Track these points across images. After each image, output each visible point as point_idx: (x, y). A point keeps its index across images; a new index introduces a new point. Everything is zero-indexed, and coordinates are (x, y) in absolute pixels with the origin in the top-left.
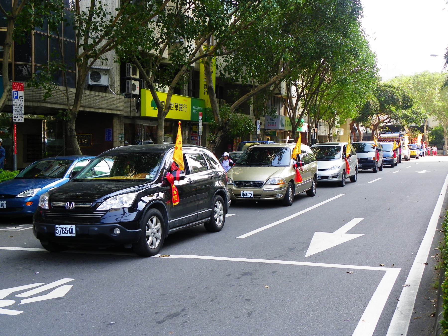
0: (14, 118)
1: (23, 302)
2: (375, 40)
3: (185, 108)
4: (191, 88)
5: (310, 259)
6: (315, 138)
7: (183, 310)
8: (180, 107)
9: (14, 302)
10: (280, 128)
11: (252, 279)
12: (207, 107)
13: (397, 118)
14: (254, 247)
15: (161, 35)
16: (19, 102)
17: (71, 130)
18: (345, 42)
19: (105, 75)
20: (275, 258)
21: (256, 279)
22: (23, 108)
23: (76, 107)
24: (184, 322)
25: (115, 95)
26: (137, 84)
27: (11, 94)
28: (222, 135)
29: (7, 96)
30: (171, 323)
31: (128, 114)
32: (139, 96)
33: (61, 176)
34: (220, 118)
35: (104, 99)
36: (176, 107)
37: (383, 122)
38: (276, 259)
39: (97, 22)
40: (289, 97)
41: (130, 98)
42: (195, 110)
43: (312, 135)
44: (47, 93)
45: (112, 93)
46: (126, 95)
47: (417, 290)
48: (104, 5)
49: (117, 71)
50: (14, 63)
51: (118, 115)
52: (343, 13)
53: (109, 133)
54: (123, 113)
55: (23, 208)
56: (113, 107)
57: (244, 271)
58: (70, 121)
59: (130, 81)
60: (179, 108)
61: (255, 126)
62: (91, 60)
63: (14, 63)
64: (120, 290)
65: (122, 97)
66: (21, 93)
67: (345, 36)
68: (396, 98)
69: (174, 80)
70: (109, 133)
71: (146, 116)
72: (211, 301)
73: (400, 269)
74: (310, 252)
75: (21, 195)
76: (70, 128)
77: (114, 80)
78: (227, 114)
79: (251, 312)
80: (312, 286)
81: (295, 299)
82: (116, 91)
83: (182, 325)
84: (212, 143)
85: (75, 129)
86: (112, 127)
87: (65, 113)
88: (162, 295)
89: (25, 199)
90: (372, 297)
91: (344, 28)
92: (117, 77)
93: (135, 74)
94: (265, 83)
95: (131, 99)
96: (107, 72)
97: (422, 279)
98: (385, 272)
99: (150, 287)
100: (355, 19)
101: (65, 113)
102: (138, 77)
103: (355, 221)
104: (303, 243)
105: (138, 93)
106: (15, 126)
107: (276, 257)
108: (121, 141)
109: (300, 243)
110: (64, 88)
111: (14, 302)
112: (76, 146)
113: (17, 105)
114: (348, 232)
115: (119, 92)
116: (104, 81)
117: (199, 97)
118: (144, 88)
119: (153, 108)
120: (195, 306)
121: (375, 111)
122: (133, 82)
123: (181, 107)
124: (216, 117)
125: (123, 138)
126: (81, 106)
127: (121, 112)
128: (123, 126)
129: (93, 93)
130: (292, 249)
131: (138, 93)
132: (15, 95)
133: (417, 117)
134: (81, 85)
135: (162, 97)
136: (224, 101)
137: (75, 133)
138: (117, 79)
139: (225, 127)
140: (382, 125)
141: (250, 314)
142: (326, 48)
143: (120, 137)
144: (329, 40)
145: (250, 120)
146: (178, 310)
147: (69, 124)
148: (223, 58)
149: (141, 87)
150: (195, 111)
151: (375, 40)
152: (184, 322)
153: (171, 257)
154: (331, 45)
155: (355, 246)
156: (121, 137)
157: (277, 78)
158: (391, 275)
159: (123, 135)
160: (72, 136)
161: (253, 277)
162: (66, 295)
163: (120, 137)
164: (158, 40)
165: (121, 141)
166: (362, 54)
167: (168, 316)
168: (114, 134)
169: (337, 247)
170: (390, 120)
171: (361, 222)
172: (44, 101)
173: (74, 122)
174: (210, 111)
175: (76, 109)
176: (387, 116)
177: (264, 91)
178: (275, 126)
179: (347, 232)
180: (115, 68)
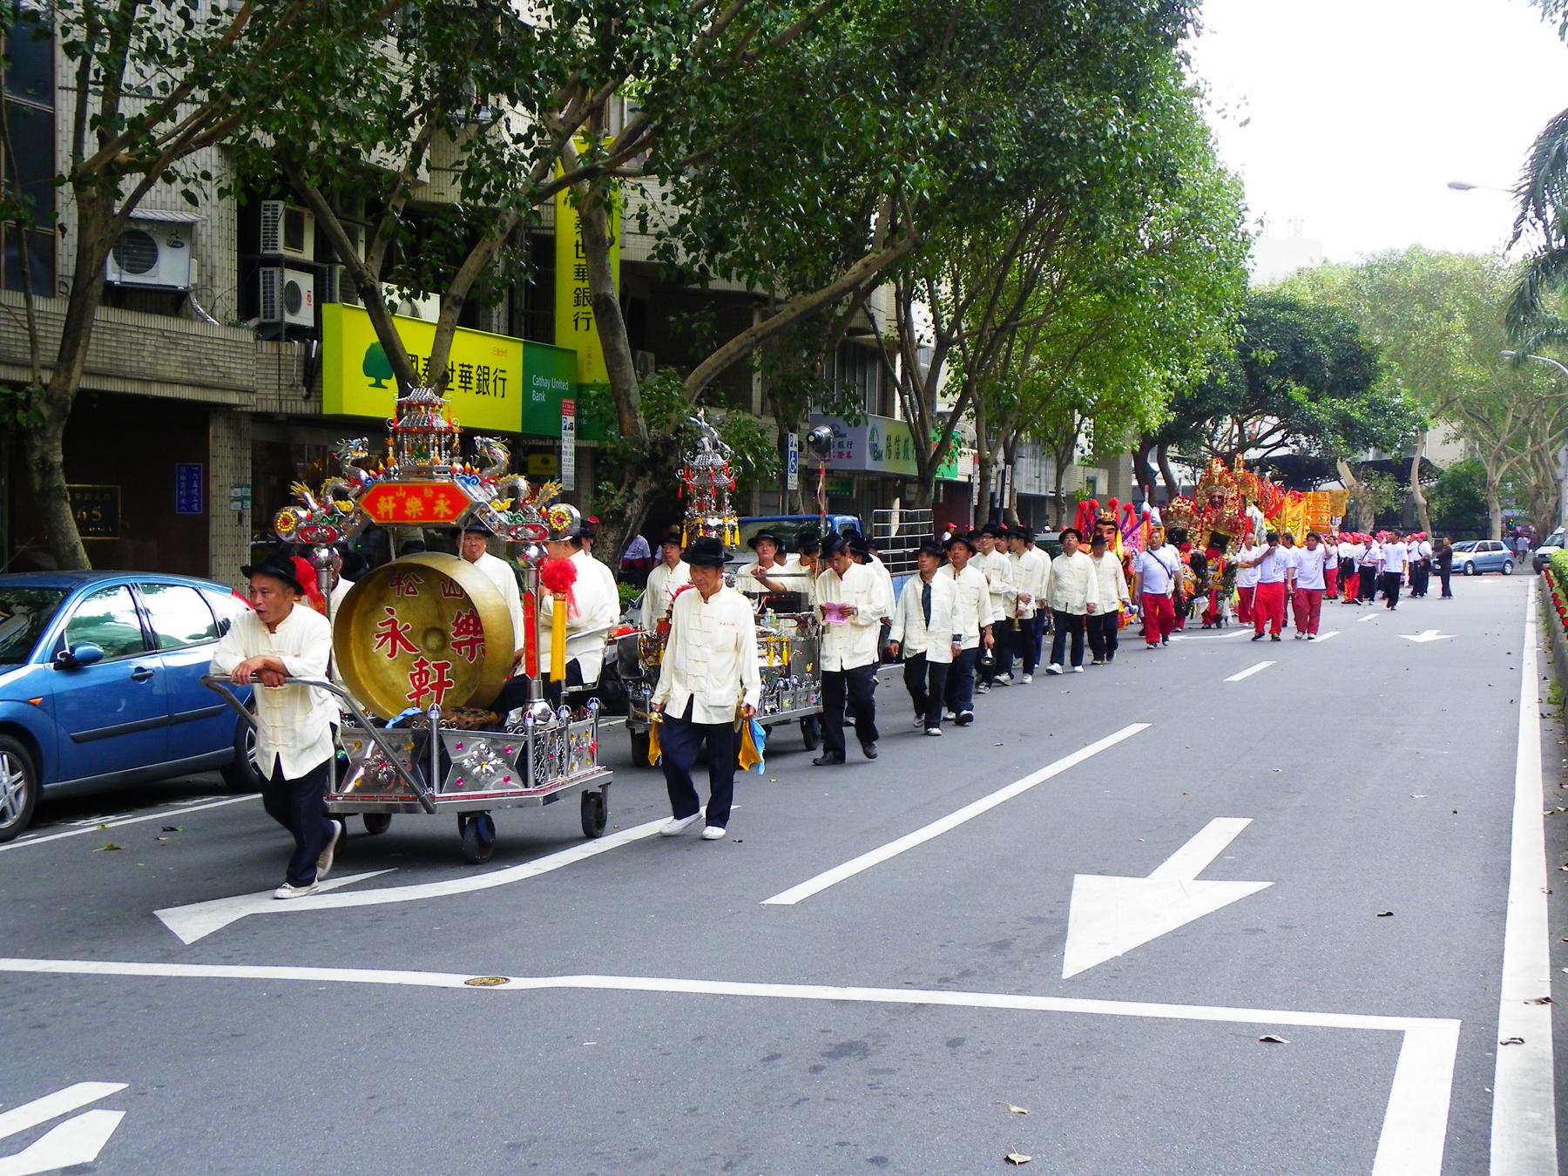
2: (1247, 121)
3: (500, 383)
5: (1085, 984)
6: (1006, 506)
8: (481, 380)
10: (870, 464)
11: (873, 1071)
12: (588, 379)
14: (839, 937)
15: (417, 88)
17: (47, 469)
18: (1135, 129)
19: (176, 245)
20: (944, 983)
21: (891, 1071)
23: (69, 371)
26: (306, 283)
28: (652, 492)
31: (270, 406)
32: (316, 332)
33: (18, 654)
34: (641, 421)
35: (172, 340)
36: (466, 378)
37: (1257, 443)
38: (948, 989)
39: (161, 27)
40: (905, 340)
41: (275, 338)
42: (539, 390)
43: (993, 495)
45: (205, 320)
47: (1553, 1109)
49: (225, 233)
51: (226, 409)
53: (189, 487)
56: (208, 375)
58: (41, 431)
59: (276, 271)
60: (474, 382)
61: (776, 459)
62: (130, 183)
64: (331, 1129)
65: (249, 337)
67: (1133, 105)
69: (462, 271)
70: (189, 482)
72: (725, 1169)
74: (1078, 957)
76: (44, 460)
77: (213, 267)
78: (671, 408)
81: (1069, 1154)
82: (219, 312)
84: (612, 522)
85: (65, 464)
86: (204, 456)
87: (21, 395)
88: (514, 1145)
90: (1381, 1142)
91: (1128, 73)
93: (295, 241)
94: (819, 286)
95: (283, 345)
96: (181, 234)
97: (1556, 1062)
98: (1399, 1035)
99: (456, 1115)
100: (1171, 41)
101: (21, 395)
102: (308, 254)
103: (1220, 833)
104: (1040, 920)
105: (310, 323)
108: (240, 515)
109: (1029, 919)
110: (16, 299)
112: (66, 535)
115: (234, 316)
116: (171, 269)
118: (331, 301)
119: (373, 381)
122: (290, 276)
123: (487, 378)
124: (627, 418)
126: (87, 373)
127: (244, 396)
128: (249, 454)
129: (130, 318)
130: (1002, 946)
131: (310, 323)
133: (1389, 424)
134: (91, 281)
135: (416, 340)
136: (651, 357)
137: (60, 480)
138: (225, 262)
139: (665, 460)
140: (1253, 454)
143: (237, 499)
144: (1074, 118)
147: (38, 442)
149: (322, 296)
150: (538, 397)
151: (1247, 121)
153: (516, 983)
154: (1083, 140)
155: (1251, 932)
156: (242, 499)
157: (866, 266)
159: (248, 492)
160: (50, 493)
162: (103, 1152)
163: (237, 499)
165: (240, 515)
166: (1192, 178)
168: (213, 487)
169: (1179, 933)
170: (1284, 438)
173: (60, 434)
174: (600, 395)
175: (68, 380)
176: (1275, 420)
177: (813, 317)
178: (849, 456)
179: (1205, 875)
180: (215, 219)
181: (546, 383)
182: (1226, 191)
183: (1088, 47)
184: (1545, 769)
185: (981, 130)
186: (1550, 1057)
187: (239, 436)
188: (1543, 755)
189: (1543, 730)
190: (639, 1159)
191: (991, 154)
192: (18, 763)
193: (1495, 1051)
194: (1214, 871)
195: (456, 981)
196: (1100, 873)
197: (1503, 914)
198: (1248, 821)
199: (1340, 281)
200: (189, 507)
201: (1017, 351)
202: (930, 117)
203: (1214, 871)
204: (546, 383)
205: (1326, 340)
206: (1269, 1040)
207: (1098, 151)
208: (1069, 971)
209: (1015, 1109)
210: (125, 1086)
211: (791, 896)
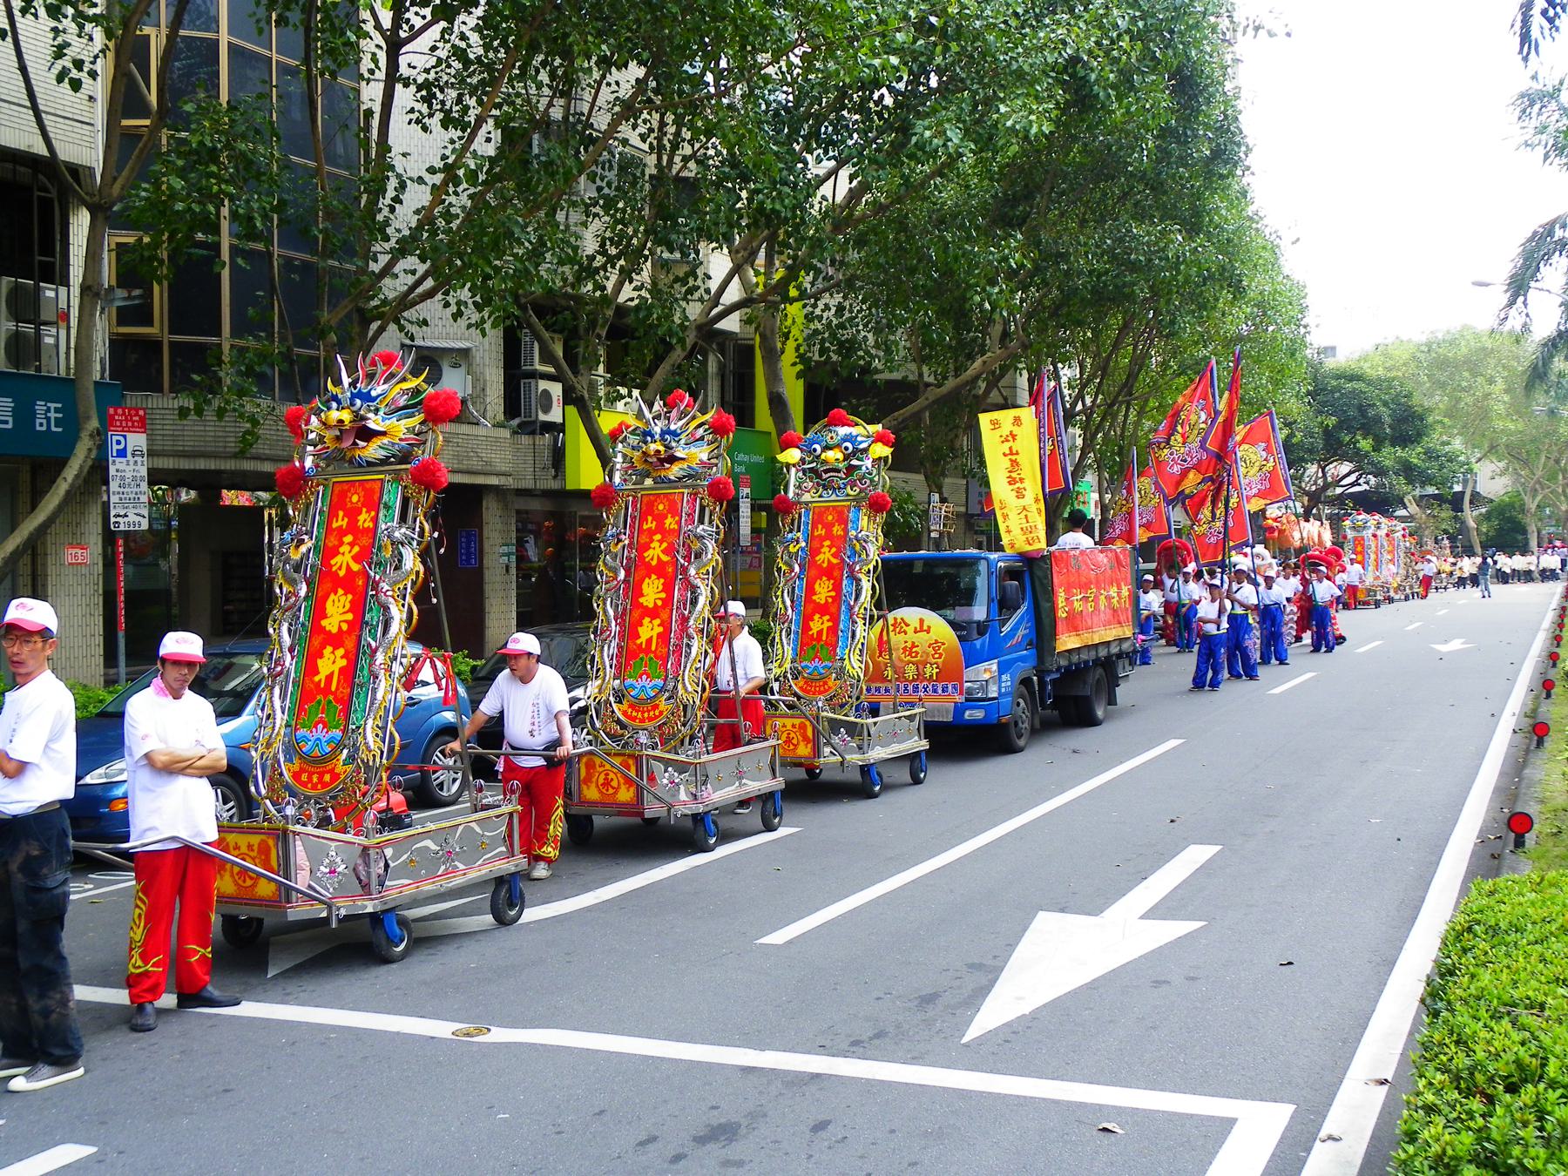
0: (113, 520)
4: (730, 397)
11: (727, 1163)
13: (1380, 472)
15: (603, 245)
16: (132, 467)
19: (456, 366)
20: (856, 1048)
21: (740, 1164)
22: (144, 486)
25: (486, 429)
26: (556, 390)
27: (103, 447)
29: (90, 450)
37: (1337, 483)
41: (533, 433)
42: (740, 463)
44: (247, 432)
46: (519, 426)
48: (404, 155)
50: (167, 338)
51: (496, 487)
52: (1182, 161)
53: (468, 543)
54: (509, 482)
55: (101, 817)
56: (475, 464)
57: (717, 1119)
59: (533, 381)
62: (374, 326)
65: (506, 433)
66: (137, 440)
67: (1193, 227)
68: (1371, 413)
71: (583, 487)
73: (1289, 1109)
74: (994, 1013)
75: (100, 776)
82: (489, 414)
89: (110, 790)
92: (494, 370)
94: (956, 376)
96: (462, 356)
98: (1230, 1123)
103: (1197, 855)
106: (121, 542)
107: (855, 1043)
109: (971, 966)
113: (123, 478)
114: (1153, 913)
116: (454, 382)
117: (752, 425)
121: (1311, 451)
122: (543, 385)
125: (513, 558)
130: (929, 999)
132: (115, 447)
133: (1441, 467)
142: (1132, 271)
143: (504, 555)
145: (909, 493)
148: (804, 306)
149: (569, 398)
153: (499, 1035)
155: (1158, 983)
156: (508, 555)
161: (736, 1150)
163: (504, 555)
164: (592, 258)
166: (1256, 285)
171: (1205, 869)
172: (240, 455)
180: (488, 349)
181: (746, 458)
183: (1157, 187)
184: (1497, 790)
185: (1061, 255)
186: (1358, 1161)
187: (506, 507)
188: (1502, 774)
189: (1511, 746)
192: (231, 796)
193: (1309, 1150)
194: (1161, 911)
195: (442, 1029)
196: (1062, 910)
197: (1391, 964)
199: (1406, 356)
200: (468, 561)
201: (1132, 416)
202: (1014, 250)
203: (1161, 911)
204: (746, 458)
205: (1385, 404)
206: (1105, 1130)
207: (1162, 269)
208: (972, 1033)
210: (89, 1150)
211: (779, 937)
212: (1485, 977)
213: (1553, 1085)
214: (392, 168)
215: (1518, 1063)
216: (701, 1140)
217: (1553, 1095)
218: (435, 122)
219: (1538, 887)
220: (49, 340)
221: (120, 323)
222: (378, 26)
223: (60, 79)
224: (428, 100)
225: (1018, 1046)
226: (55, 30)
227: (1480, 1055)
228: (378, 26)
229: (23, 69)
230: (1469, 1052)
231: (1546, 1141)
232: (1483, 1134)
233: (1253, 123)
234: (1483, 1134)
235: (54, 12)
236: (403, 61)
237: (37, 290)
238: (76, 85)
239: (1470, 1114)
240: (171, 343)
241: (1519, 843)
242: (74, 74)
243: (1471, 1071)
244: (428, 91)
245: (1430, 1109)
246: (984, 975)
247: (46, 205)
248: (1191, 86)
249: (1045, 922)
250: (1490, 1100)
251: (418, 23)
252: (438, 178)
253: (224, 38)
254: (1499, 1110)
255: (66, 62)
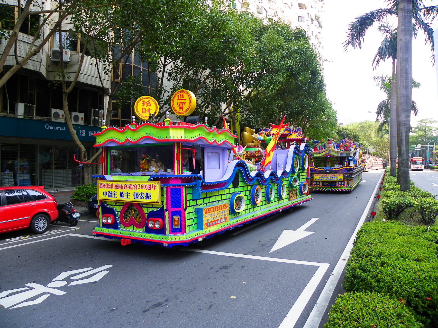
1: (72, 284)
7: (166, 300)
9: (66, 283)
11: (226, 272)
20: (250, 253)
21: (228, 273)
24: (161, 312)
30: (152, 313)
57: (224, 265)
63: (121, 120)
67: (315, 101)
74: (275, 248)
79: (212, 305)
80: (264, 280)
83: (158, 316)
88: (160, 284)
100: (321, 91)
103: (314, 220)
104: (273, 239)
107: (250, 253)
111: (66, 283)
114: (306, 230)
120: (176, 297)
130: (263, 245)
141: (210, 307)
146: (162, 300)
152: (161, 312)
155: (306, 243)
158: (323, 267)
161: (228, 270)
164: (200, 105)
167: (153, 305)
182: (334, 113)
183: (308, 92)
184: (370, 208)
190: (177, 289)
191: (292, 108)
194: (306, 230)
198: (318, 218)
208: (271, 251)
209: (244, 282)
212: (364, 239)
213: (373, 256)
214: (164, 89)
215: (368, 253)
216: (221, 268)
217: (373, 258)
218: (172, 80)
219: (374, 224)
220: (100, 120)
221: (112, 117)
222: (161, 62)
223: (105, 73)
224: (170, 76)
225: (280, 253)
226: (104, 64)
227: (362, 251)
228: (161, 62)
229: (98, 71)
230: (360, 251)
231: (371, 265)
232: (361, 264)
233: (326, 81)
234: (361, 264)
235: (104, 61)
236: (166, 68)
237: (98, 111)
238: (107, 74)
239: (359, 261)
240: (122, 121)
241: (373, 217)
242: (107, 72)
243: (360, 254)
244: (170, 74)
245: (352, 260)
246: (274, 241)
247: (100, 95)
248: (315, 74)
249: (285, 232)
250: (363, 259)
251: (169, 62)
252: (172, 90)
253: (133, 65)
254: (364, 260)
255: (106, 70)
